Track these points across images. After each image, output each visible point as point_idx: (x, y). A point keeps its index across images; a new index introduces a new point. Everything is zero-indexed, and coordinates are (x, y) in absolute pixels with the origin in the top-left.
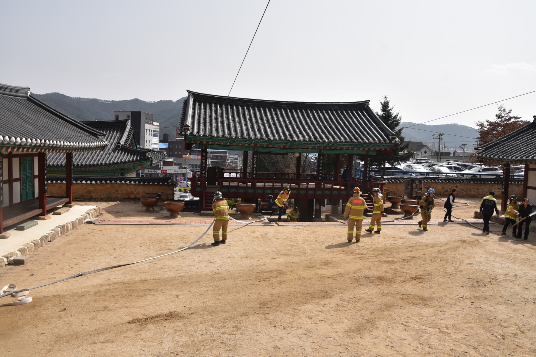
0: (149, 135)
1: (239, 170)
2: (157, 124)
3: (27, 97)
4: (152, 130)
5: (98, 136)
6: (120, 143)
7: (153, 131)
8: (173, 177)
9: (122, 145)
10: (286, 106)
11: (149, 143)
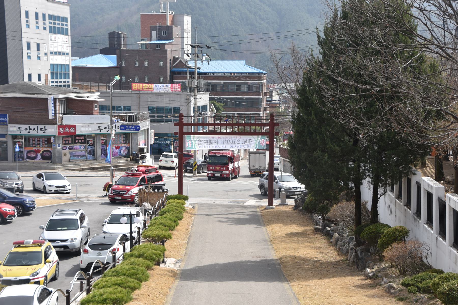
0: (38, 27)
1: (265, 125)
4: (44, 15)
7: (50, 17)
8: (93, 144)
11: (38, 49)
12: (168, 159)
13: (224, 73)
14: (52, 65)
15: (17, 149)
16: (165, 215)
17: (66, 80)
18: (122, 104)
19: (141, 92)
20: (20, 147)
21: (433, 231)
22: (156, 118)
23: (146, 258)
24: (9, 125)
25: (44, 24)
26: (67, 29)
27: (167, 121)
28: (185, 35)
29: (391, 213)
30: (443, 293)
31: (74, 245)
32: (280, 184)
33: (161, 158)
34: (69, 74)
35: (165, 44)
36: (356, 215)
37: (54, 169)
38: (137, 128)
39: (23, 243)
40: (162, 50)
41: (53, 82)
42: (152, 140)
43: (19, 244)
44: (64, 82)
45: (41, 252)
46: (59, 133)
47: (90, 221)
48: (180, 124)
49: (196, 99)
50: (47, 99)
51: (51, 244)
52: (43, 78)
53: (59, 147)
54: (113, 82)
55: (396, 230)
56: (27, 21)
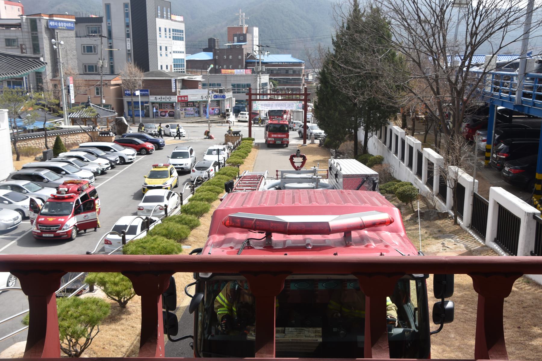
0: (166, 37)
2: (180, 18)
4: (170, 29)
7: (173, 30)
11: (166, 50)
12: (244, 116)
13: (278, 62)
14: (174, 59)
15: (155, 111)
16: (240, 150)
17: (183, 68)
18: (216, 83)
19: (227, 75)
20: (156, 109)
21: (398, 158)
22: (236, 91)
23: (227, 175)
24: (150, 96)
25: (170, 35)
26: (183, 37)
27: (243, 92)
28: (255, 39)
29: (375, 147)
30: (399, 193)
31: (187, 167)
32: (311, 131)
33: (239, 115)
34: (184, 64)
36: (354, 149)
37: (176, 122)
38: (224, 97)
39: (157, 166)
40: (241, 49)
41: (175, 70)
42: (234, 104)
43: (155, 166)
44: (181, 69)
45: (168, 171)
46: (178, 101)
47: (196, 153)
48: (250, 94)
49: (260, 78)
50: (171, 80)
51: (174, 167)
52: (169, 68)
53: (178, 109)
54: (209, 69)
55: (377, 157)
56: (160, 33)
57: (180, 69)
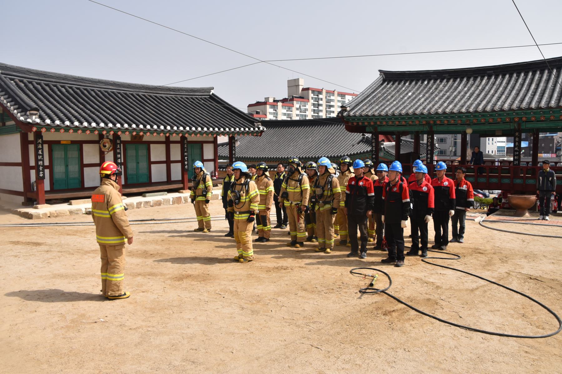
3: (210, 95)
5: (255, 123)
6: (365, 135)
9: (367, 137)
10: (492, 72)
14: (498, 147)
34: (505, 150)
35: (553, 136)
57: (501, 153)
